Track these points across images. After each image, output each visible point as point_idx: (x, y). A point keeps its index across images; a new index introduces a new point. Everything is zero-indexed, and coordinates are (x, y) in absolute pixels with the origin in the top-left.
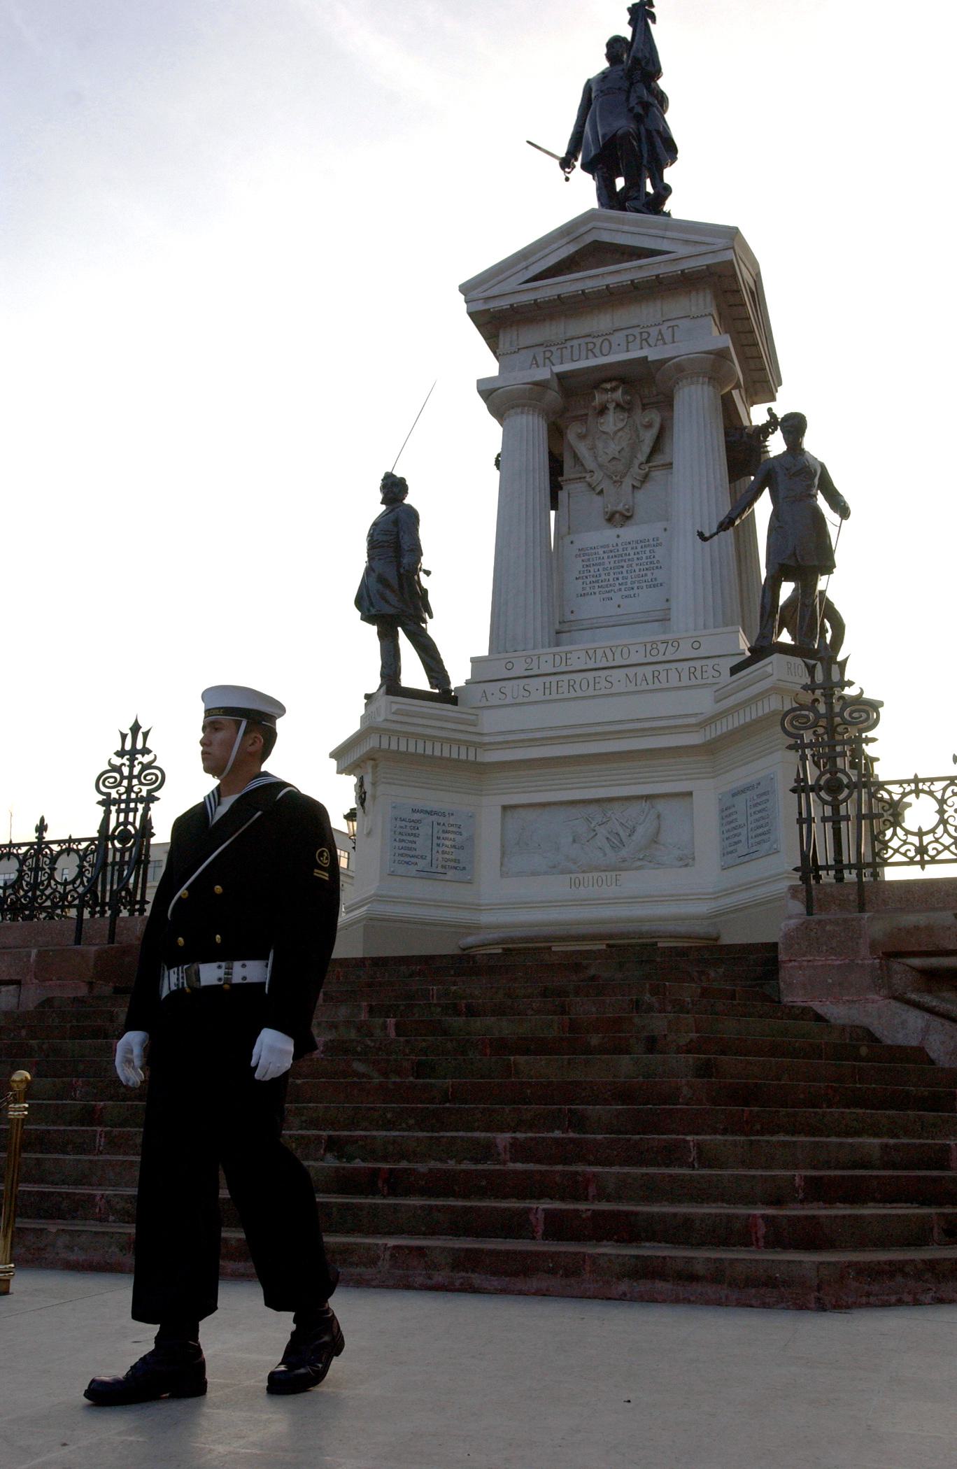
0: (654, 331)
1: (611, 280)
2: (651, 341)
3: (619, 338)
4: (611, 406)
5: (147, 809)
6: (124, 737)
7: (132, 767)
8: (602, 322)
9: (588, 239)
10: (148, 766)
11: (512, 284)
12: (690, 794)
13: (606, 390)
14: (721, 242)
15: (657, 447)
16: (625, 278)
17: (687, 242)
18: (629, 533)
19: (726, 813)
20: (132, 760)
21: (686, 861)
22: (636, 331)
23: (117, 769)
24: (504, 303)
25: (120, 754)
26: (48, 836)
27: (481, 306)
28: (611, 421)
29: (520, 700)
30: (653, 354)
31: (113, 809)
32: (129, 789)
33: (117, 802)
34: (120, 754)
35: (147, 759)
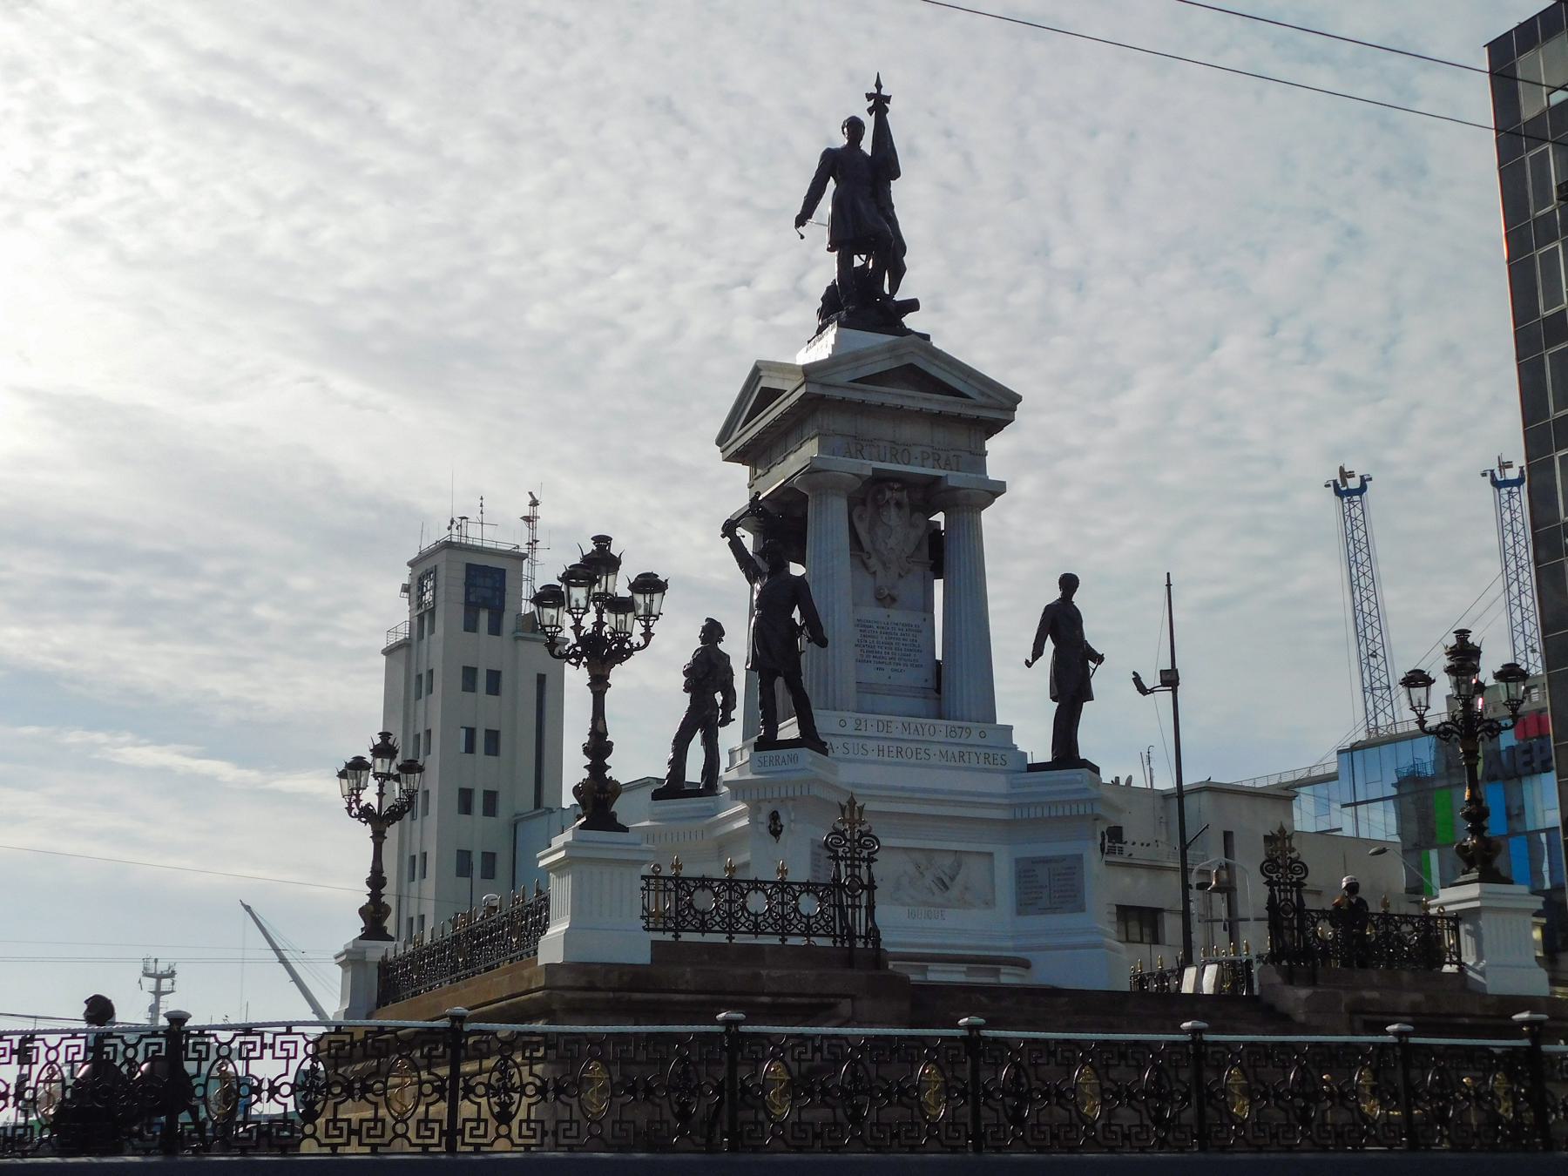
0: (943, 455)
1: (926, 406)
2: (942, 463)
3: (916, 451)
4: (892, 503)
5: (869, 868)
6: (843, 809)
7: (852, 834)
8: (909, 432)
9: (907, 360)
10: (867, 834)
11: (842, 378)
12: (990, 854)
13: (892, 489)
14: (1008, 404)
15: (918, 547)
16: (936, 408)
17: (983, 394)
18: (896, 615)
19: (1026, 872)
20: (852, 828)
21: (989, 903)
22: (930, 450)
23: (842, 834)
24: (837, 394)
25: (843, 822)
26: (789, 878)
27: (816, 390)
28: (893, 517)
29: (859, 756)
30: (954, 478)
31: (842, 864)
32: (852, 850)
33: (842, 858)
34: (843, 822)
35: (864, 828)
